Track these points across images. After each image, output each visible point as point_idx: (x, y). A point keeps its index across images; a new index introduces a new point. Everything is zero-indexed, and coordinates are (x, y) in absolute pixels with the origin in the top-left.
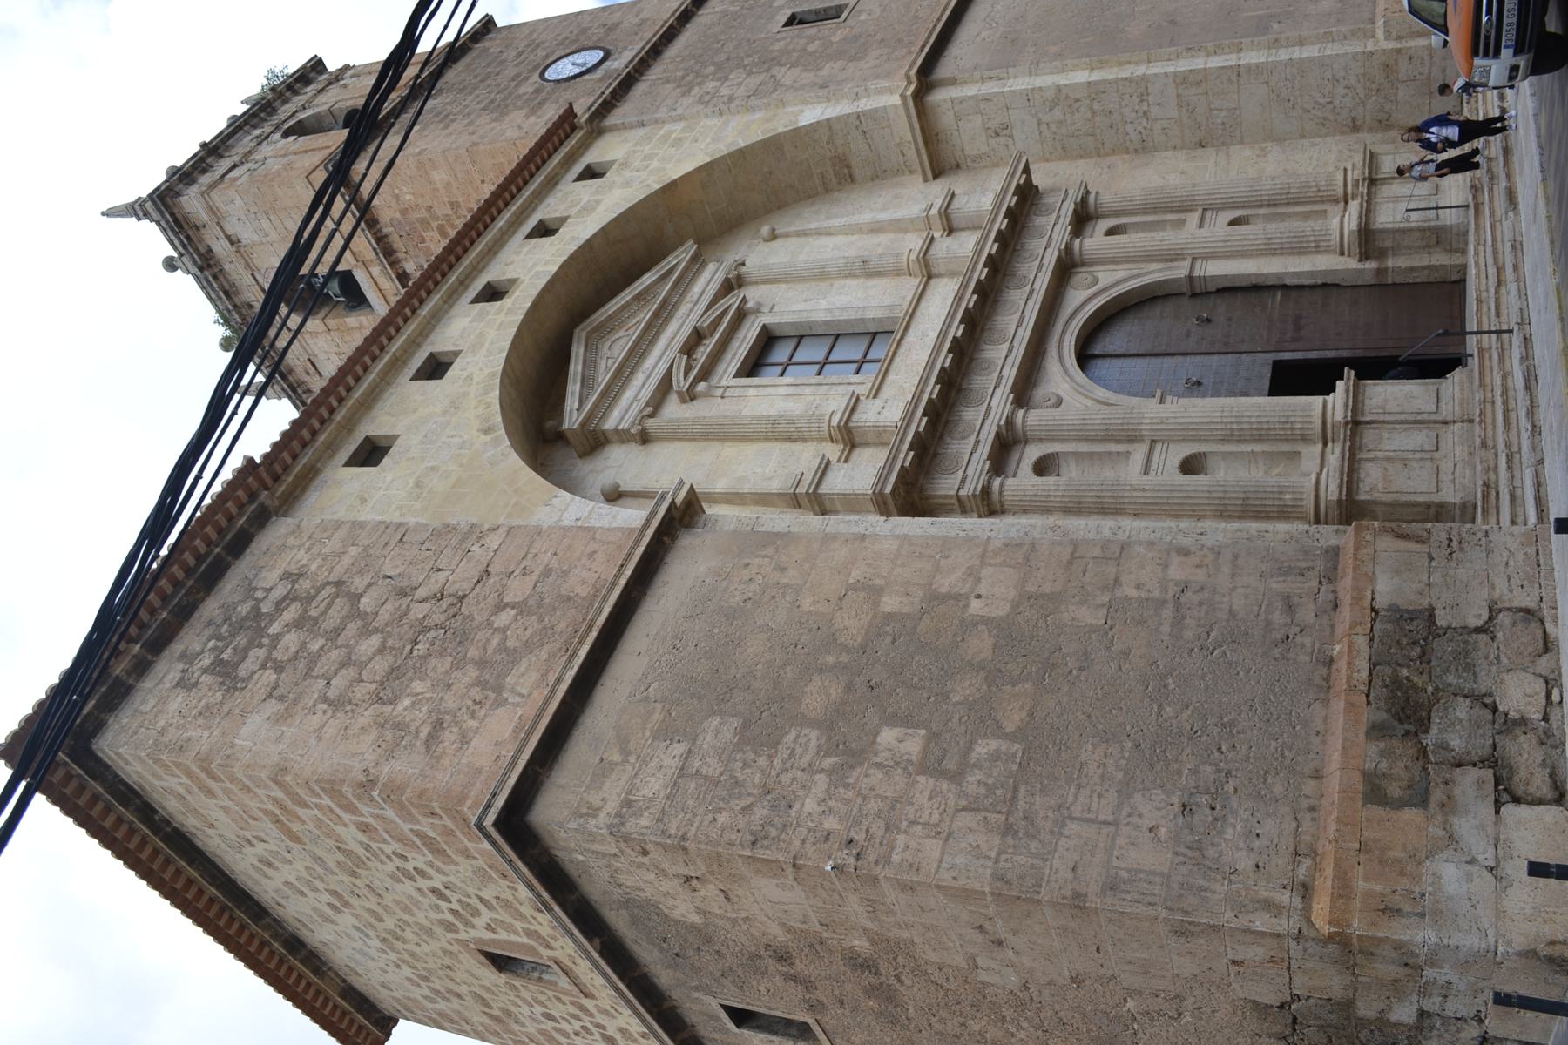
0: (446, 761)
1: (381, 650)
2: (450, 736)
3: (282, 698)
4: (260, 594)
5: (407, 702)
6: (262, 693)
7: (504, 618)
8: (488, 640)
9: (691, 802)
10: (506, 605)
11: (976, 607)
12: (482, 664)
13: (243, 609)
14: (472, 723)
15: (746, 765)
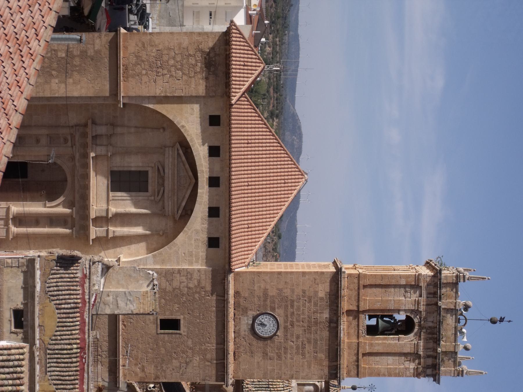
1: (167, 62)
2: (140, 45)
3: (184, 48)
4: (210, 73)
5: (154, 51)
6: (190, 48)
7: (144, 72)
8: (145, 66)
9: (90, 40)
10: (145, 75)
11: (57, 81)
12: (143, 61)
13: (212, 69)
14: (137, 48)
15: (84, 47)
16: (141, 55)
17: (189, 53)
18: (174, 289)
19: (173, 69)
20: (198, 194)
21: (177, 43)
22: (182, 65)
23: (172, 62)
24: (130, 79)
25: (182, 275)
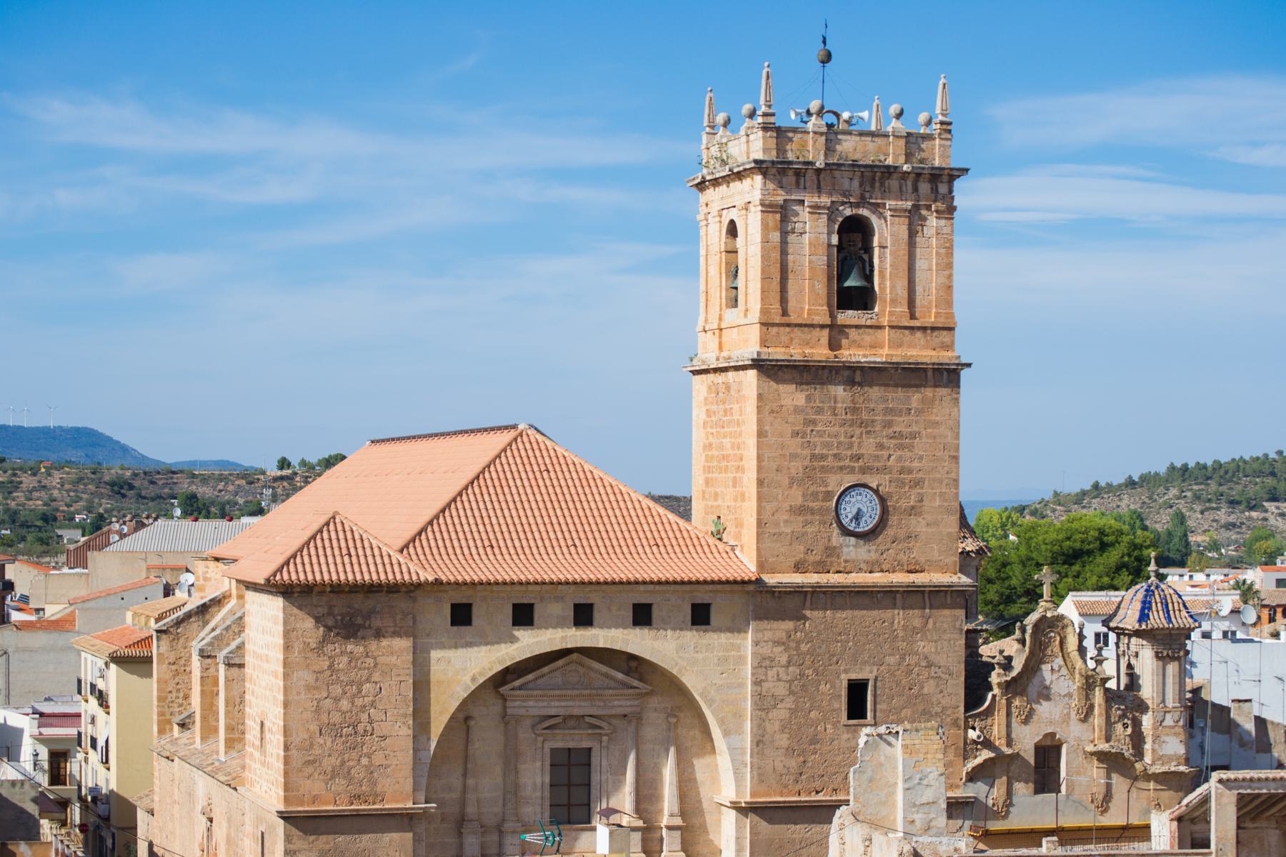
0: (300, 774)
2: (310, 770)
3: (317, 680)
4: (367, 625)
5: (322, 742)
6: (317, 668)
7: (364, 761)
12: (343, 763)
13: (359, 621)
16: (330, 768)
17: (326, 668)
18: (792, 693)
19: (359, 702)
20: (608, 646)
21: (305, 694)
22: (351, 683)
23: (345, 704)
24: (379, 789)
25: (764, 678)
